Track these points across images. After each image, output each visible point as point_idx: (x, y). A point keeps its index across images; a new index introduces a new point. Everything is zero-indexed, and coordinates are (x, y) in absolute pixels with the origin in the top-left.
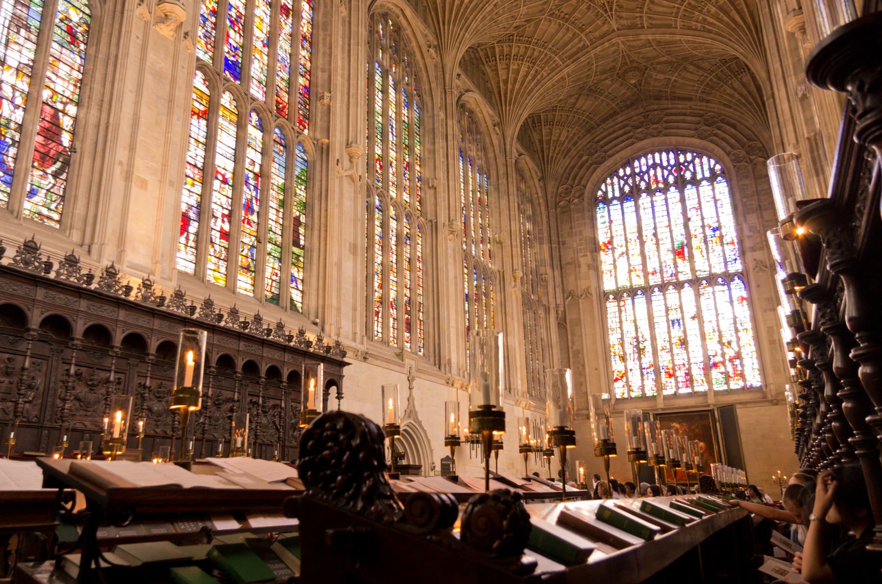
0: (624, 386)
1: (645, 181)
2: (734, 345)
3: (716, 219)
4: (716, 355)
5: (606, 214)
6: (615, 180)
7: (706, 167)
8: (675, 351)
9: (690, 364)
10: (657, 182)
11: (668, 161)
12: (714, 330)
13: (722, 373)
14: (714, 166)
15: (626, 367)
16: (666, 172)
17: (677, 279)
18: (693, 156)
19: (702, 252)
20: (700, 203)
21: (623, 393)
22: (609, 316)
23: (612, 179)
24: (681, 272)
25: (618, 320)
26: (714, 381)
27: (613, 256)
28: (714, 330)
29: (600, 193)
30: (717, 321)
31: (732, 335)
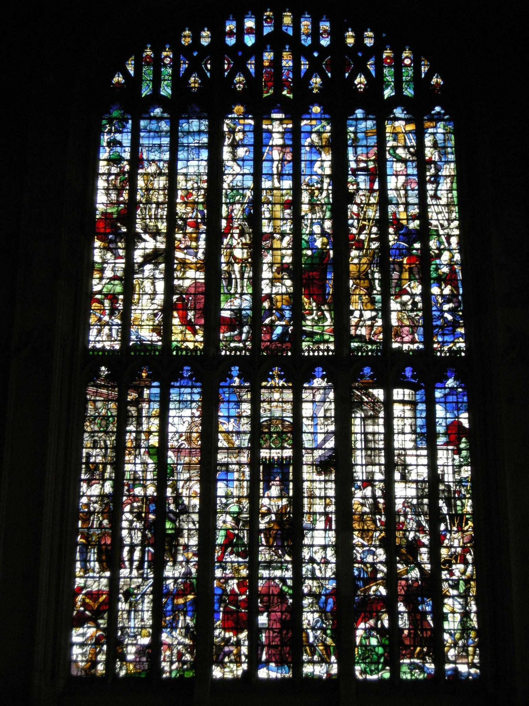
0: (98, 642)
1: (246, 73)
2: (424, 556)
3: (414, 210)
4: (372, 579)
5: (126, 139)
6: (167, 54)
7: (408, 74)
8: (264, 555)
9: (298, 595)
10: (279, 84)
11: (315, 34)
12: (376, 504)
13: (382, 631)
14: (429, 75)
15: (114, 581)
16: (305, 66)
17: (297, 349)
18: (376, 38)
19: (370, 289)
20: (381, 160)
21: (94, 663)
22: (89, 427)
23: (157, 51)
24: (311, 334)
25: (110, 441)
26: (358, 651)
27: (129, 257)
28: (376, 504)
29: (119, 79)
30: (389, 483)
31: (420, 528)
